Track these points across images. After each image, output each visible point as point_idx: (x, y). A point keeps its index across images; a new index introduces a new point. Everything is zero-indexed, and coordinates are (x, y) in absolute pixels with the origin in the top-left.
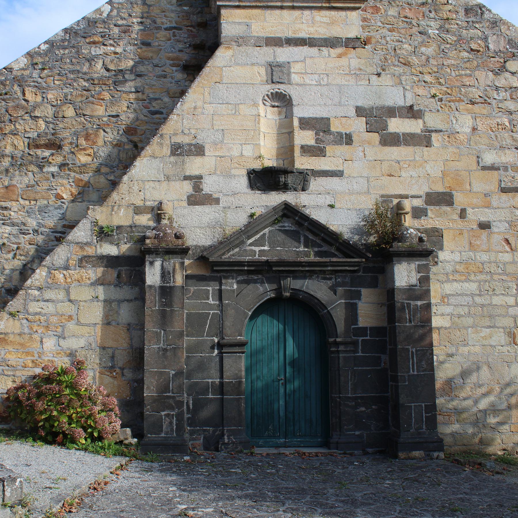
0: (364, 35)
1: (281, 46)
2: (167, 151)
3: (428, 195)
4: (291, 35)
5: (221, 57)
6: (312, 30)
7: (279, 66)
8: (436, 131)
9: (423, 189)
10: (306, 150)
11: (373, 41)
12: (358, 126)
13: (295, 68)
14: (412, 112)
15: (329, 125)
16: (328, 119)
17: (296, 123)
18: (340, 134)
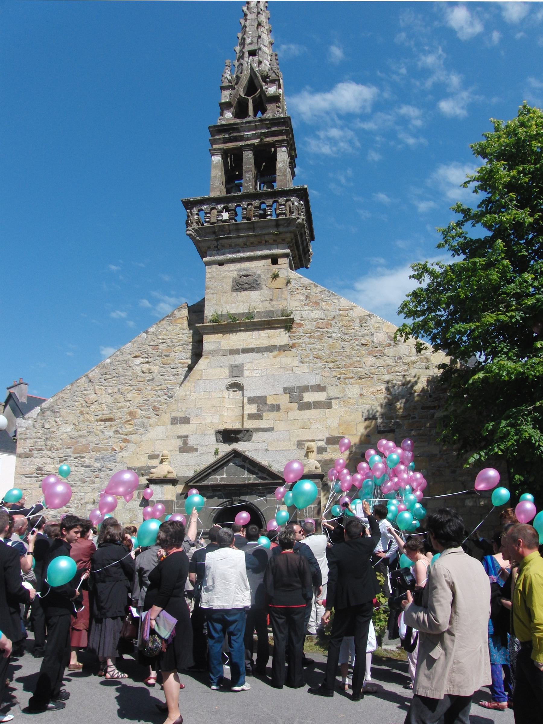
0: (291, 342)
1: (239, 354)
2: (168, 421)
3: (327, 438)
4: (245, 346)
5: (202, 363)
6: (258, 342)
7: (236, 366)
8: (335, 398)
9: (325, 436)
10: (251, 417)
11: (297, 345)
12: (284, 400)
13: (246, 367)
14: (320, 388)
15: (266, 400)
16: (266, 397)
17: (246, 400)
18: (273, 405)
